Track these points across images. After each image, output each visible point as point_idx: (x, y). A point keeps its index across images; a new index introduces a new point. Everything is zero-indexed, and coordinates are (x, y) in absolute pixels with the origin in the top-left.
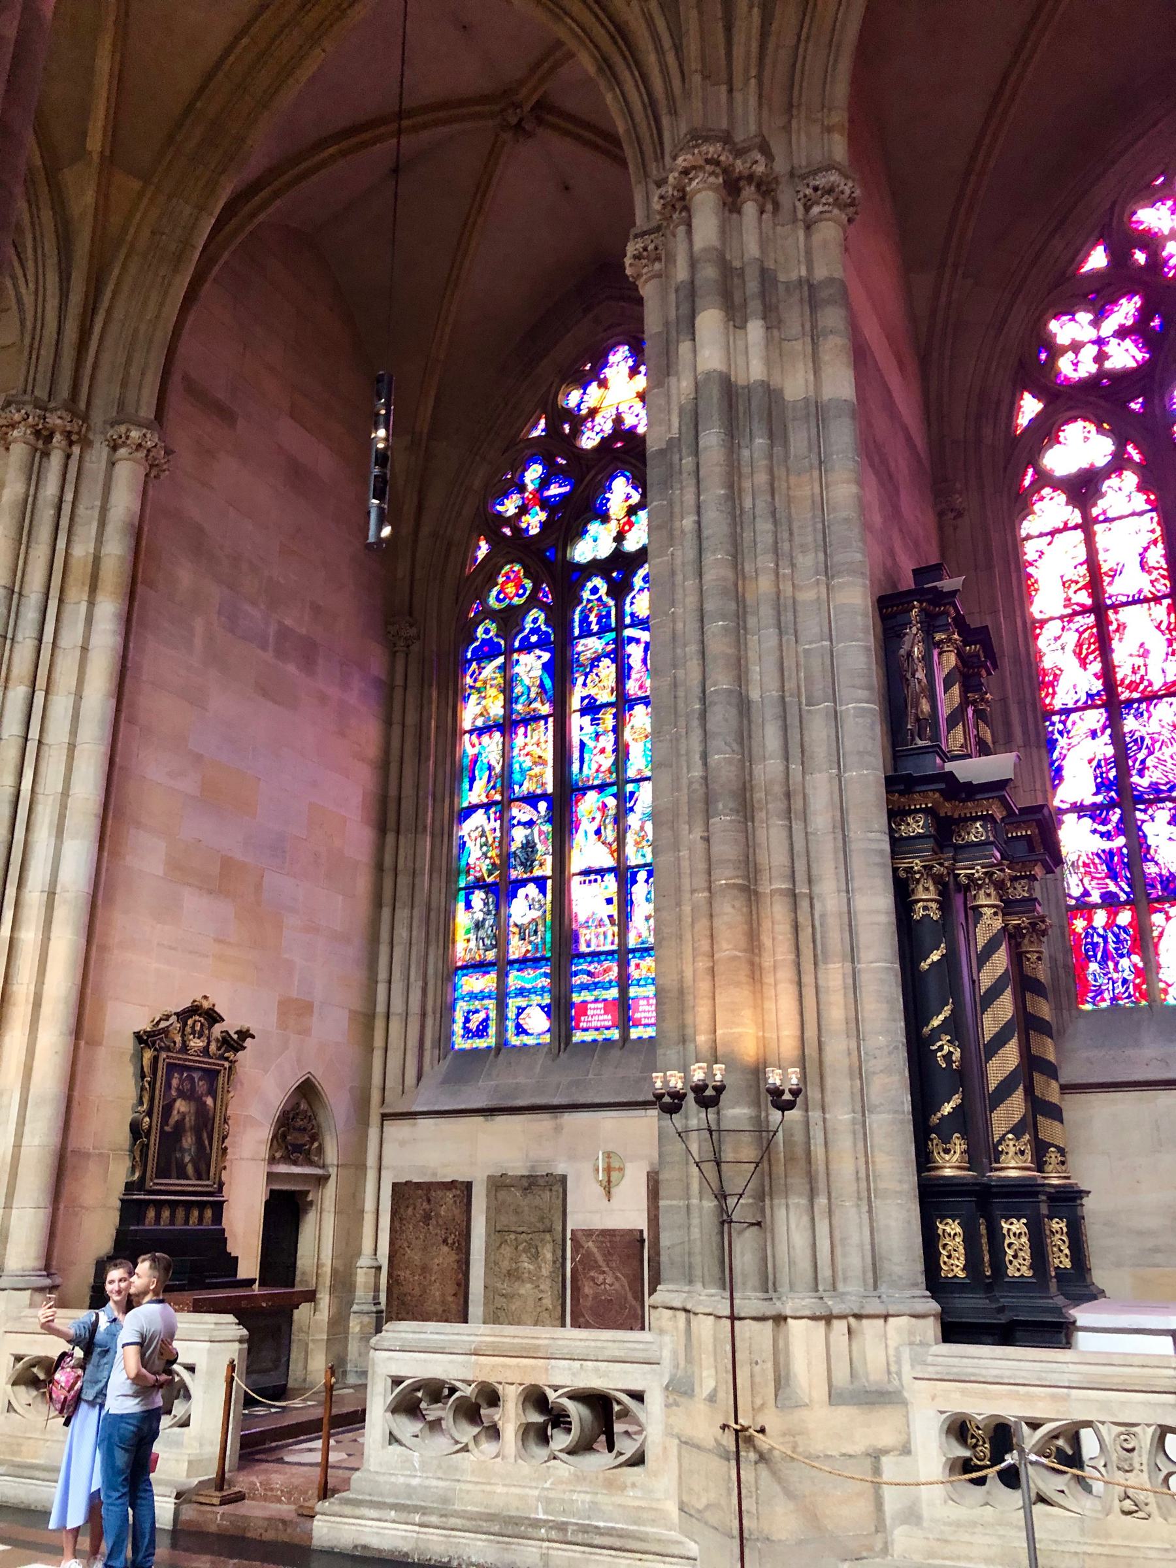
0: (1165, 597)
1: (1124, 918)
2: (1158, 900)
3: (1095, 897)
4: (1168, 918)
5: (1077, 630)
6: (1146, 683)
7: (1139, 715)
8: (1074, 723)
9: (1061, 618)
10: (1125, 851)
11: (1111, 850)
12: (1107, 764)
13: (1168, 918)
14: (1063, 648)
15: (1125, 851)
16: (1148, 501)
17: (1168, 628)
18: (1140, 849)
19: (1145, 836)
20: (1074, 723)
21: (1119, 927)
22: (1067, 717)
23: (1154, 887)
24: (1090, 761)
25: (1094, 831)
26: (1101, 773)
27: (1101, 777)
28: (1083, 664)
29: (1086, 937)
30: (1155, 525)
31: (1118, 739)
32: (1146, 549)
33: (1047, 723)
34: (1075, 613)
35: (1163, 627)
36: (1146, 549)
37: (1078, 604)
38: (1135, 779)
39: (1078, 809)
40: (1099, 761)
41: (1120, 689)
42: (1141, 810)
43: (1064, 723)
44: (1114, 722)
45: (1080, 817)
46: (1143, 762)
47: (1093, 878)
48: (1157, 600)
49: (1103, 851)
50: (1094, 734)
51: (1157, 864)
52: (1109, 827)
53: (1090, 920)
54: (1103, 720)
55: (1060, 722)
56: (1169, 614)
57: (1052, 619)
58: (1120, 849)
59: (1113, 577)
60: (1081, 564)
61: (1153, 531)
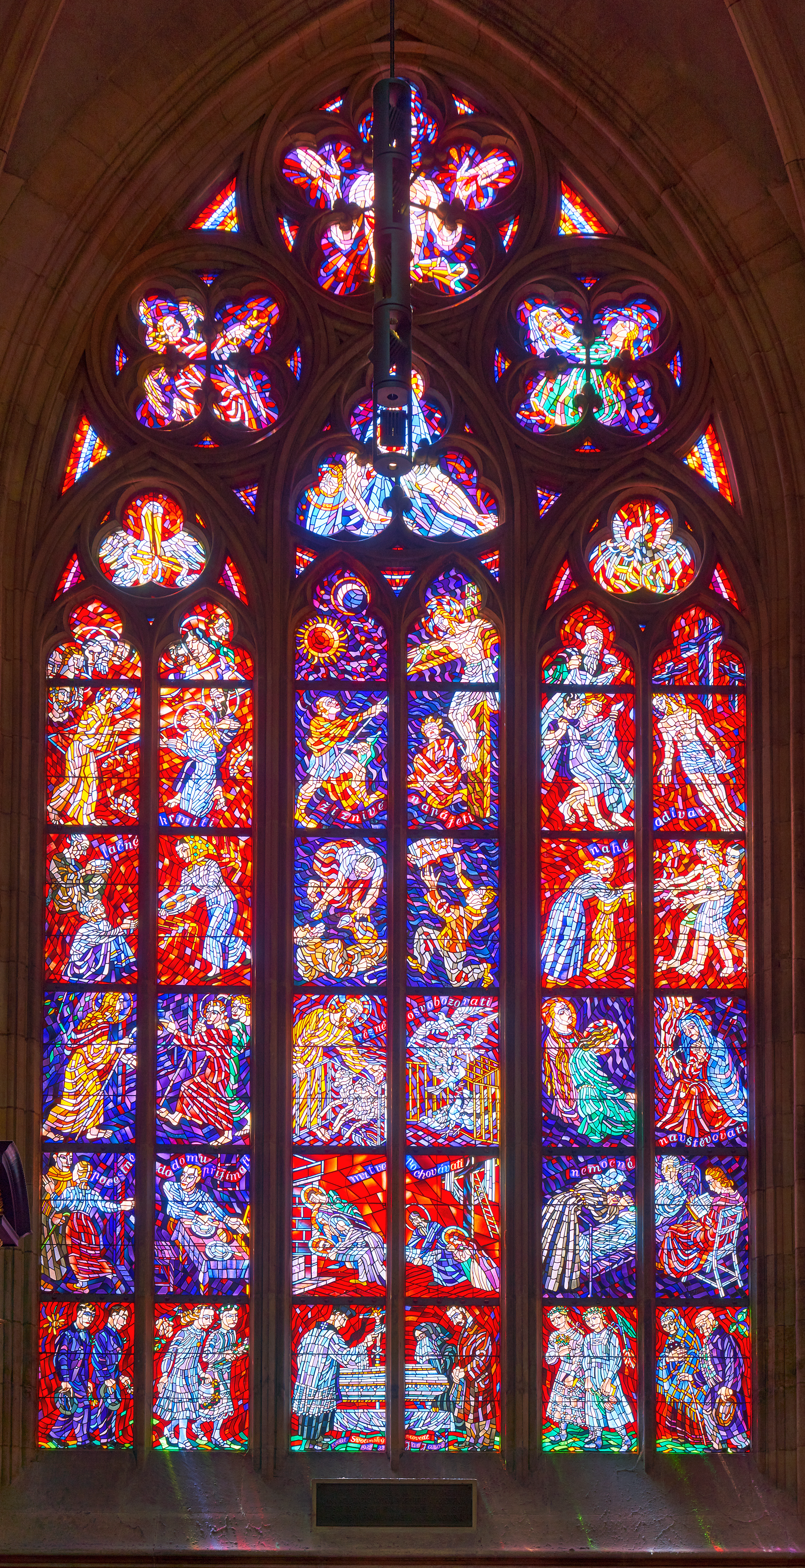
0: (243, 831)
1: (118, 1320)
2: (170, 1299)
3: (82, 1284)
4: (178, 1327)
5: (111, 858)
6: (198, 964)
7: (179, 1014)
8: (87, 1009)
9: (90, 831)
10: (132, 1219)
11: (114, 1214)
12: (124, 1084)
13: (178, 1327)
14: (86, 884)
15: (132, 1219)
16: (241, 668)
17: (240, 882)
18: (154, 1220)
19: (165, 1201)
20: (87, 1009)
21: (109, 1332)
22: (78, 999)
23: (165, 1279)
24: (102, 1074)
25: (93, 1184)
26: (116, 1095)
27: (115, 1102)
28: (114, 916)
29: (61, 1343)
30: (245, 710)
31: (146, 1046)
32: (228, 748)
33: (48, 1003)
34: (111, 830)
35: (236, 878)
36: (228, 748)
37: (117, 813)
38: (163, 1112)
39: (76, 1144)
40: (116, 1075)
41: (160, 967)
42: (163, 1162)
43: (72, 1005)
44: (144, 1020)
45: (75, 1161)
46: (176, 1087)
47: (83, 1255)
48: (232, 834)
49: (103, 1215)
50: (112, 1032)
51: (174, 1245)
52: (116, 1181)
53: (71, 1317)
54: (128, 1011)
55: (68, 1003)
56: (244, 861)
57: (79, 829)
58: (126, 1214)
59: (175, 781)
60: (132, 748)
61: (242, 720)
